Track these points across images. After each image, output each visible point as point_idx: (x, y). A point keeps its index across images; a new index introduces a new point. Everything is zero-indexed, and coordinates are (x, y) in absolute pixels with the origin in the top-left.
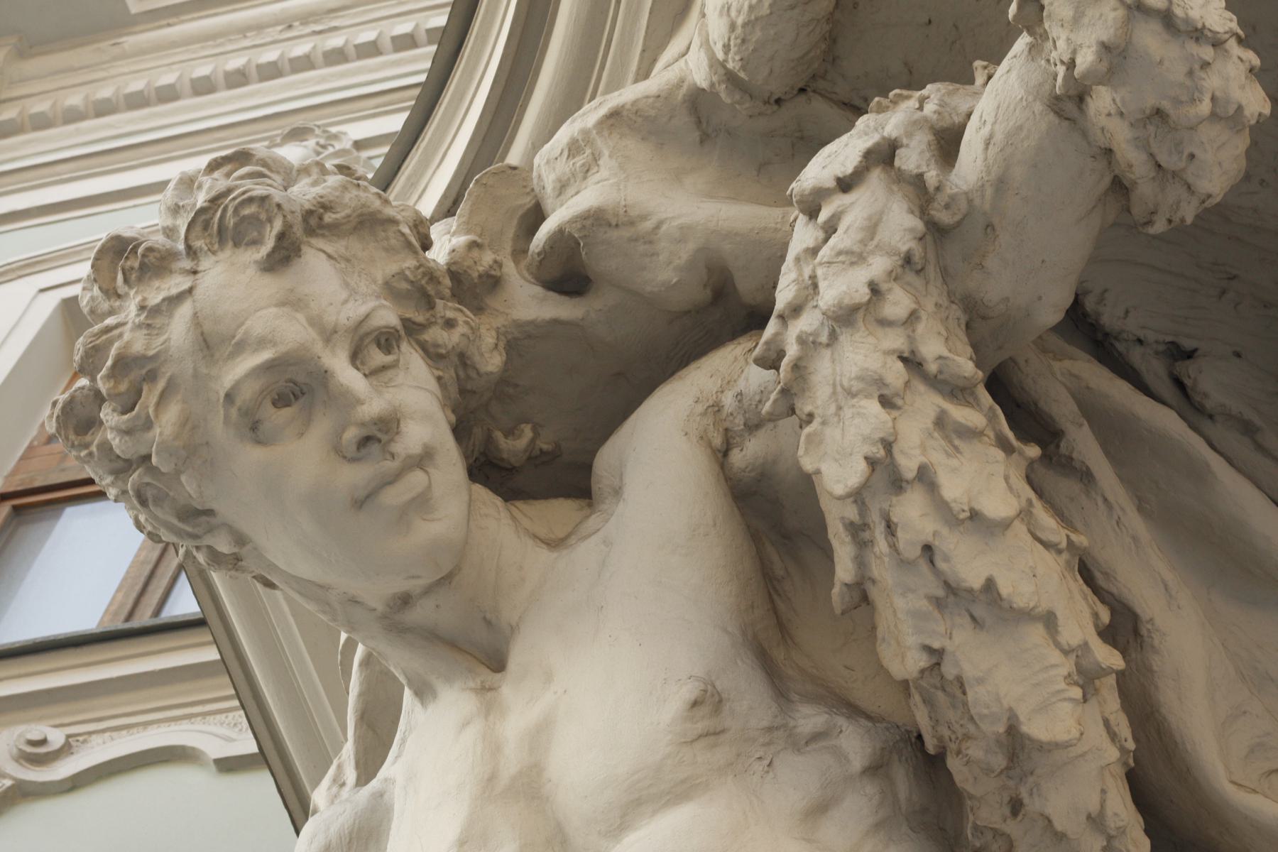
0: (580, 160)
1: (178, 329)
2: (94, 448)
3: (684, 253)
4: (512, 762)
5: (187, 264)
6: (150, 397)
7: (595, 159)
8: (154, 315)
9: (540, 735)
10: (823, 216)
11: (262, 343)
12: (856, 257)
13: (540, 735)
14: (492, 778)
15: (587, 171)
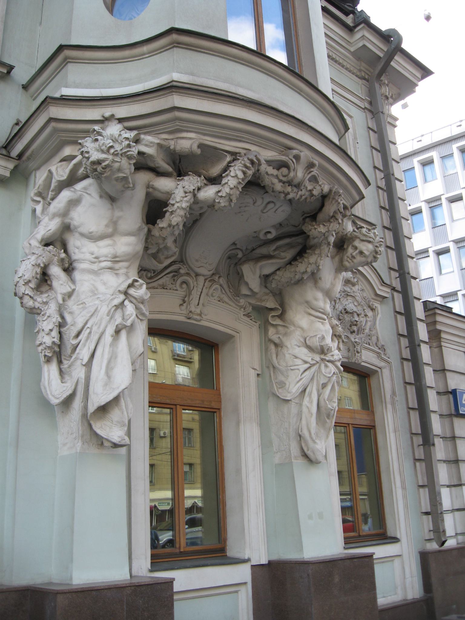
0: (151, 145)
1: (116, 165)
2: (95, 167)
3: (157, 165)
4: (115, 219)
5: (120, 156)
6: (107, 170)
7: (153, 146)
8: (114, 161)
9: (119, 218)
10: (187, 195)
11: (125, 174)
12: (187, 202)
13: (119, 218)
14: (111, 220)
15: (151, 146)
